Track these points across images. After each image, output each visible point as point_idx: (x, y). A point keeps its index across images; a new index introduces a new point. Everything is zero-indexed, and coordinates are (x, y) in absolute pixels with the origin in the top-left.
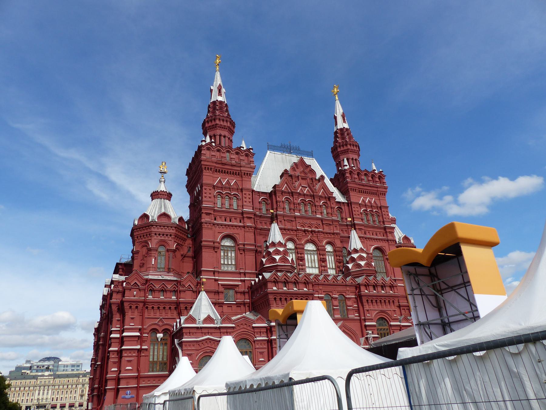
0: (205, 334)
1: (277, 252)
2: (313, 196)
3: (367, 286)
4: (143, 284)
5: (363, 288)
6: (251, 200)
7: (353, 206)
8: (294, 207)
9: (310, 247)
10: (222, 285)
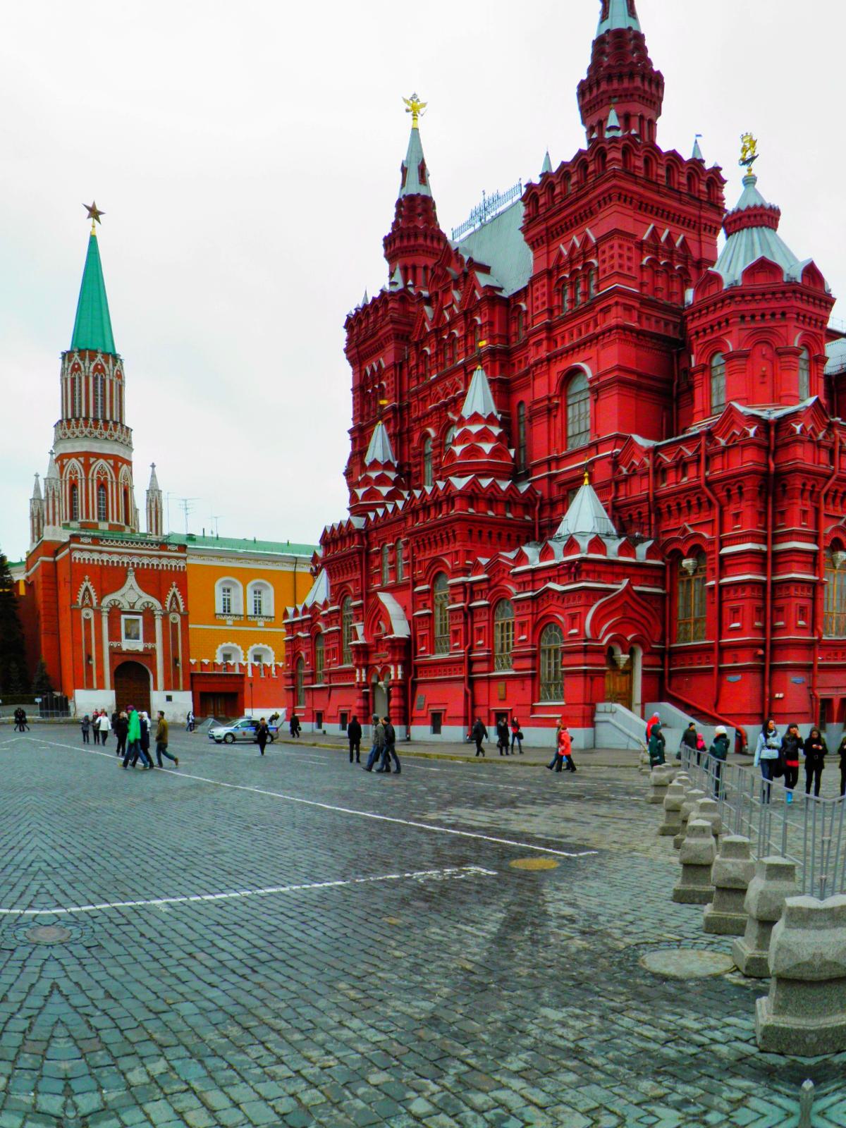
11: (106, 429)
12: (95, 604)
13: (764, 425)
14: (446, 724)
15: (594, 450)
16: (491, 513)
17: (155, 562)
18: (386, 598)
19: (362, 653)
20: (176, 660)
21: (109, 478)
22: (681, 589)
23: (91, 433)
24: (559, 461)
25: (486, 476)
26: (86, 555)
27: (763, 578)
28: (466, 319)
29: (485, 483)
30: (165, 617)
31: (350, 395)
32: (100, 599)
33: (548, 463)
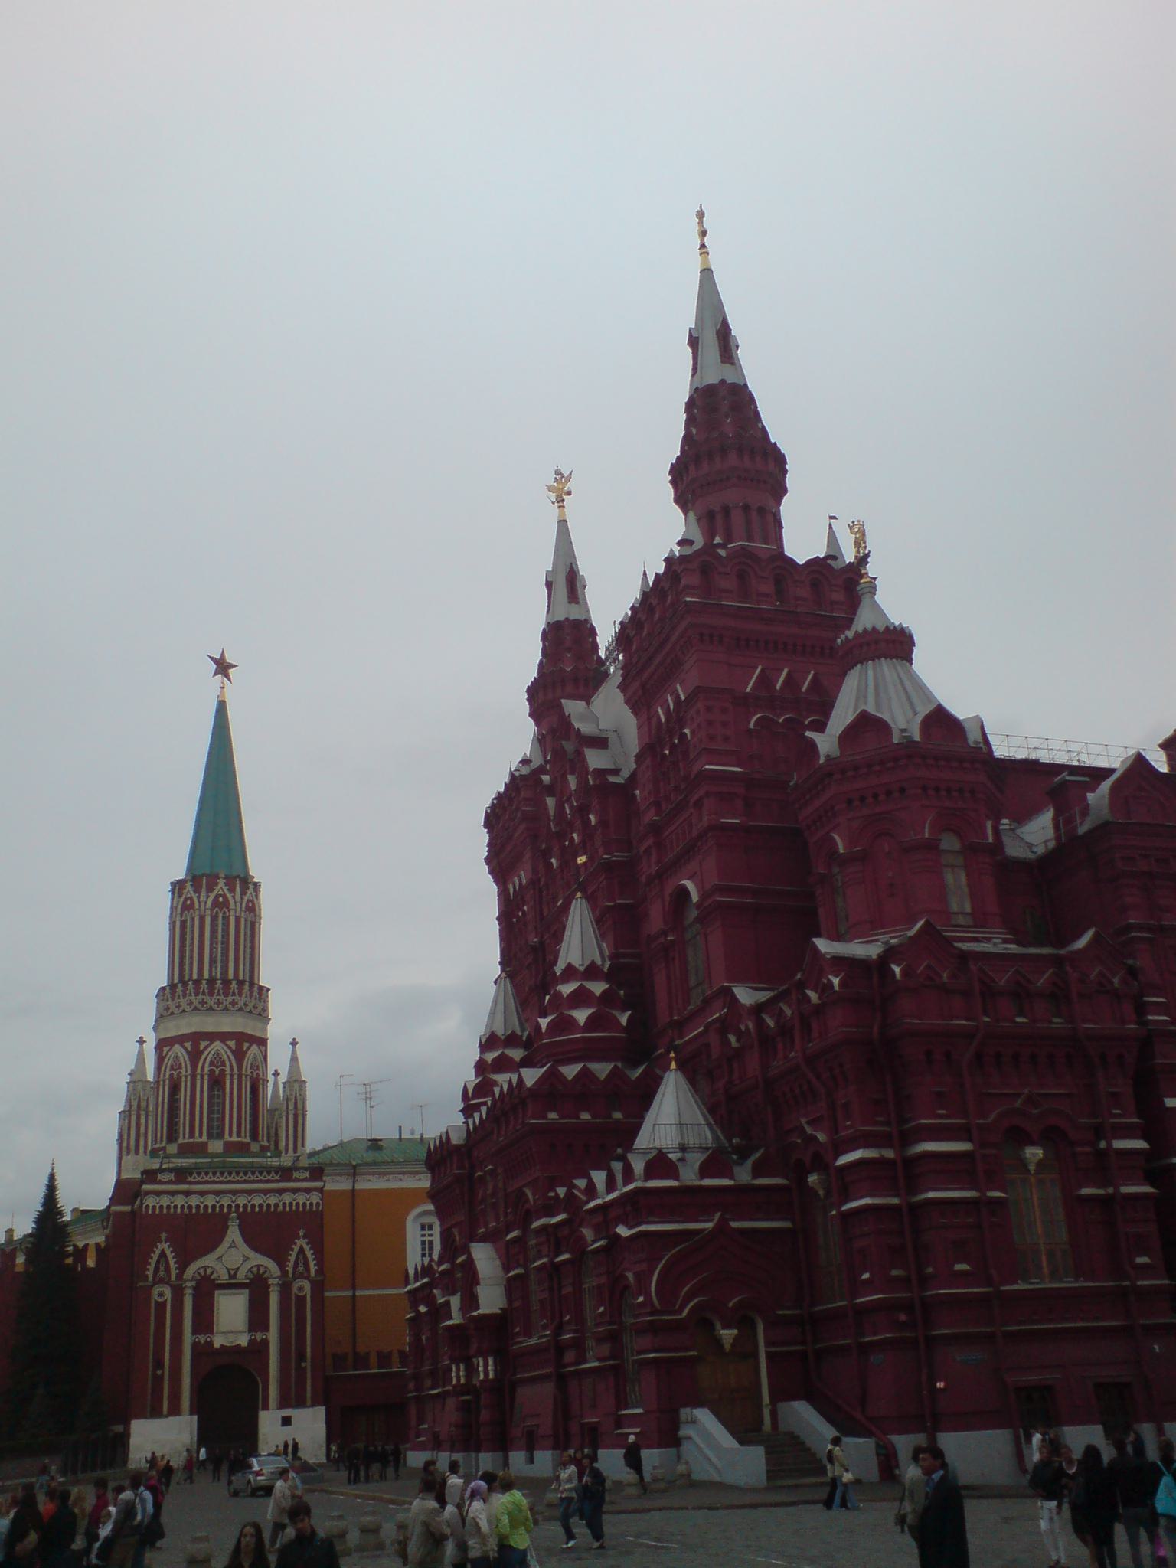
11: (226, 994)
12: (173, 1277)
16: (585, 1116)
20: (301, 1356)
21: (228, 1071)
25: (570, 1060)
26: (165, 1201)
27: (896, 1201)
29: (570, 1071)
31: (495, 928)
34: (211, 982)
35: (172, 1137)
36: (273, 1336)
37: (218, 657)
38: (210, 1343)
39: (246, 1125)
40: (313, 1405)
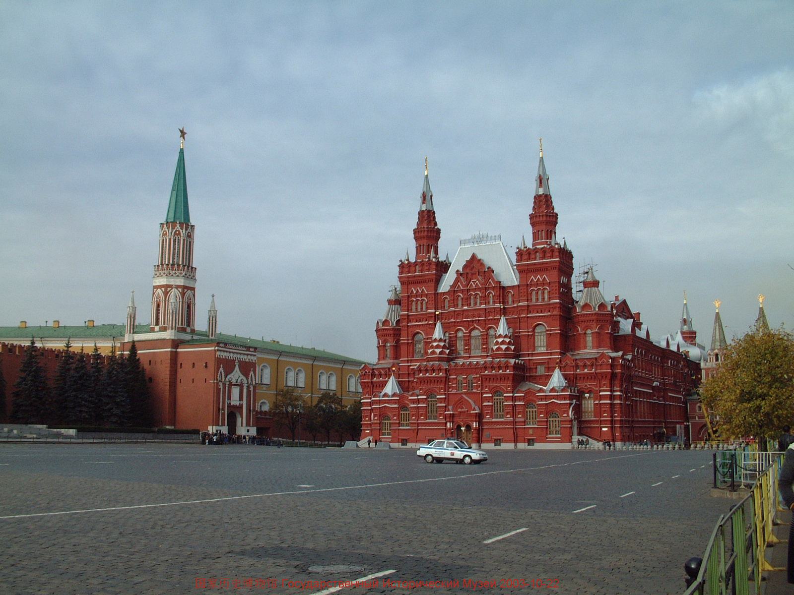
0: (384, 404)
1: (432, 347)
2: (480, 288)
3: (486, 368)
4: (369, 372)
5: (483, 370)
6: (433, 302)
7: (520, 288)
8: (467, 301)
9: (475, 333)
10: (412, 369)
13: (613, 359)
14: (503, 443)
15: (550, 354)
17: (245, 357)
18: (464, 396)
19: (452, 416)
22: (583, 402)
23: (175, 273)
24: (532, 355)
28: (485, 290)
30: (248, 387)
32: (226, 377)
33: (529, 354)
34: (173, 265)
35: (157, 324)
36: (244, 403)
37: (182, 129)
38: (230, 403)
39: (185, 322)
40: (253, 426)
